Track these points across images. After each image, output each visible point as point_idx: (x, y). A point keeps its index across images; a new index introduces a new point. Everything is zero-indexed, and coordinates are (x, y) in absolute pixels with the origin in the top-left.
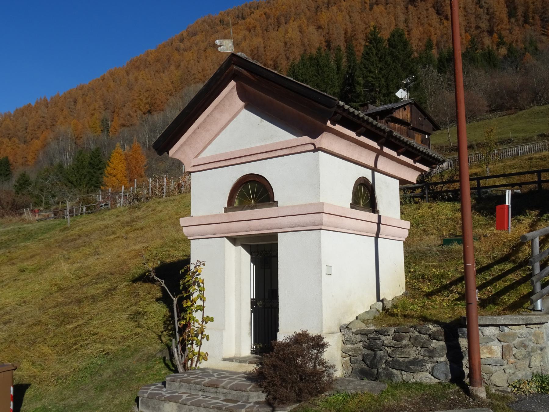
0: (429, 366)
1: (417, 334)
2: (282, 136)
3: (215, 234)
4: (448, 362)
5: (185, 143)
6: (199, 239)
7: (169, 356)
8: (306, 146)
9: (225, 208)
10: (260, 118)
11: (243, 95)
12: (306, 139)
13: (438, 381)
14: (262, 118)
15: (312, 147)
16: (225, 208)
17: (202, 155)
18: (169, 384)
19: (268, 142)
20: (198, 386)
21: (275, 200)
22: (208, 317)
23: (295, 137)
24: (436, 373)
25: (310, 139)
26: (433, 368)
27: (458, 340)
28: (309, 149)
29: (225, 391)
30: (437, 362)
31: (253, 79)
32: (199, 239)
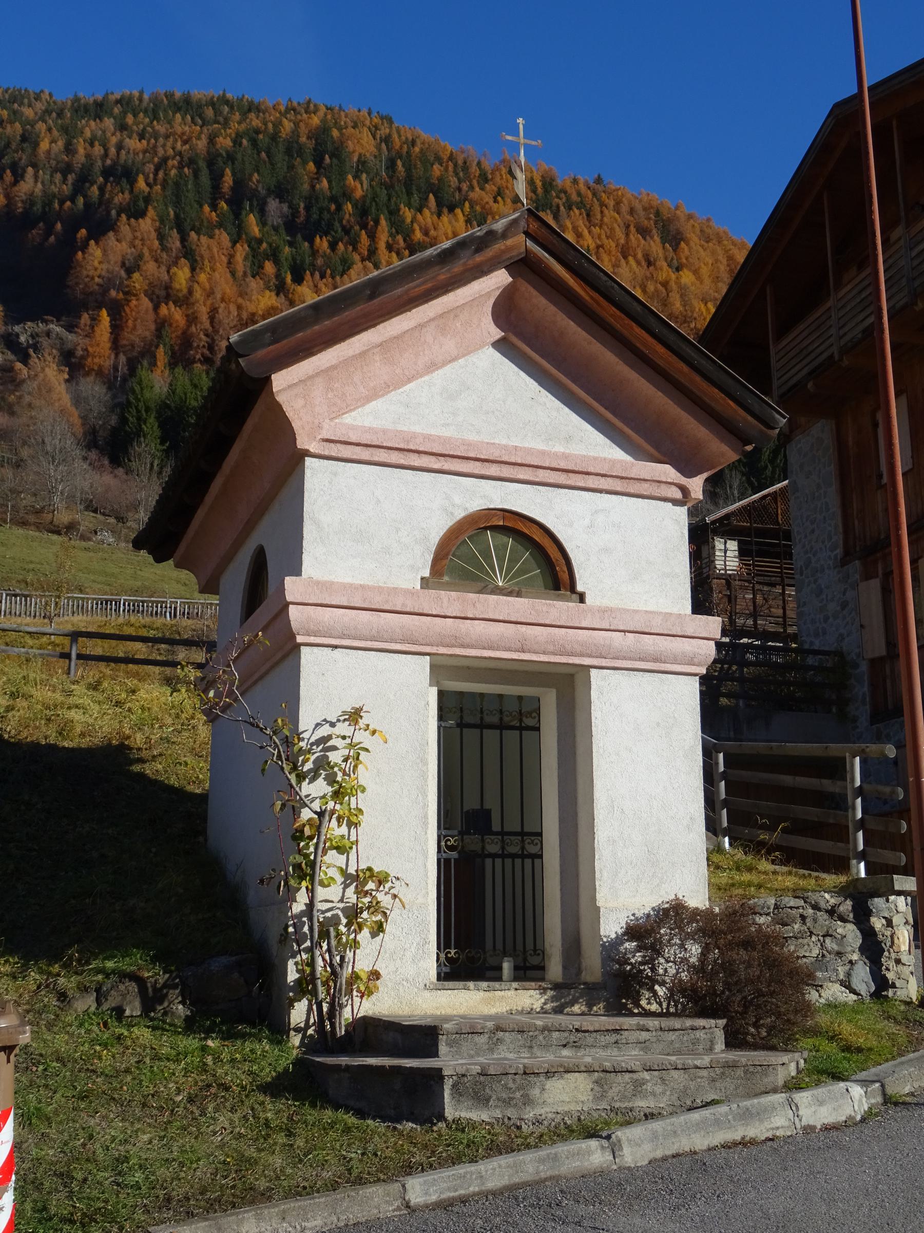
0: (842, 971)
1: (811, 911)
2: (591, 444)
3: (403, 641)
4: (867, 961)
5: (326, 372)
6: (336, 647)
7: (137, 1003)
8: (663, 486)
9: (422, 579)
10: (536, 384)
11: (506, 311)
12: (668, 472)
13: (855, 997)
14: (541, 384)
15: (678, 495)
16: (422, 579)
17: (348, 419)
18: (449, 1044)
19: (559, 448)
20: (555, 1035)
21: (580, 588)
22: (370, 869)
23: (629, 458)
24: (857, 984)
25: (679, 475)
26: (848, 975)
27: (869, 921)
28: (669, 495)
29: (644, 1035)
30: (851, 962)
31: (582, 293)
32: (336, 647)
